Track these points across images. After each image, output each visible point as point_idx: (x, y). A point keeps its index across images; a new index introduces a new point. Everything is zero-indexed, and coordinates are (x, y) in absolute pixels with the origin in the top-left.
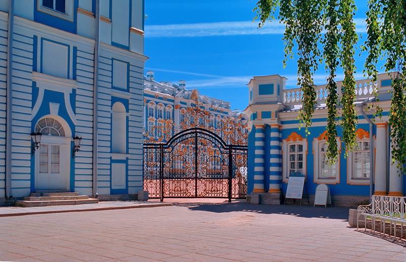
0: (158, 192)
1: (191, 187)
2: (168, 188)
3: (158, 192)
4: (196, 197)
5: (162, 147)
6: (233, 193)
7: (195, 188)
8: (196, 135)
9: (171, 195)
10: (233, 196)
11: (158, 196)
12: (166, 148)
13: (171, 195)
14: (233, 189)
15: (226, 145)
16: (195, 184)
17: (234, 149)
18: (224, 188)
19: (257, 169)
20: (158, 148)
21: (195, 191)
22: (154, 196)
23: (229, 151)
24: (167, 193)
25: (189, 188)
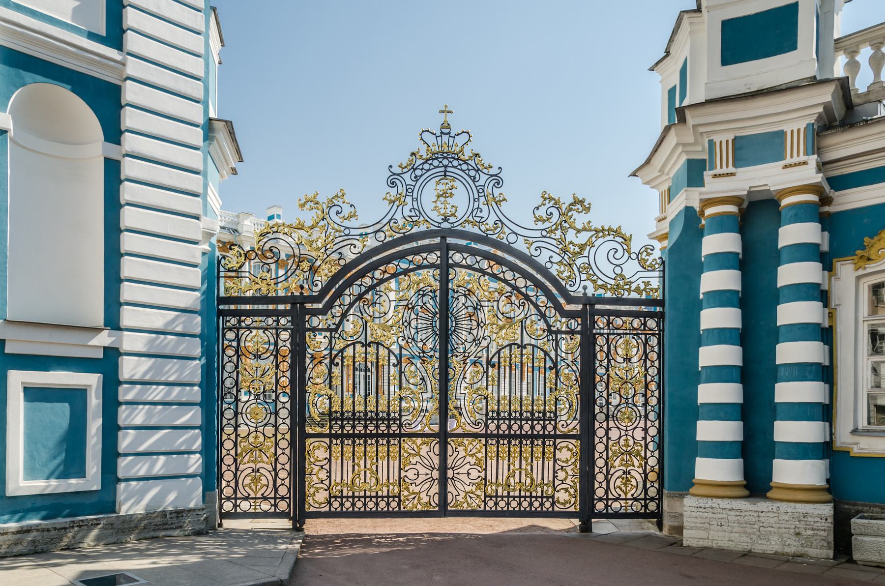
0: (283, 491)
1: (423, 471)
2: (323, 475)
3: (283, 491)
4: (443, 510)
5: (299, 308)
6: (600, 493)
7: (436, 474)
8: (445, 257)
9: (336, 504)
10: (600, 506)
11: (283, 506)
12: (315, 313)
13: (336, 504)
14: (600, 477)
15: (570, 300)
16: (436, 461)
17: (603, 313)
18: (561, 475)
19: (709, 393)
20: (284, 313)
21: (435, 488)
22: (265, 506)
23: (583, 324)
24: (317, 498)
25: (411, 474)
